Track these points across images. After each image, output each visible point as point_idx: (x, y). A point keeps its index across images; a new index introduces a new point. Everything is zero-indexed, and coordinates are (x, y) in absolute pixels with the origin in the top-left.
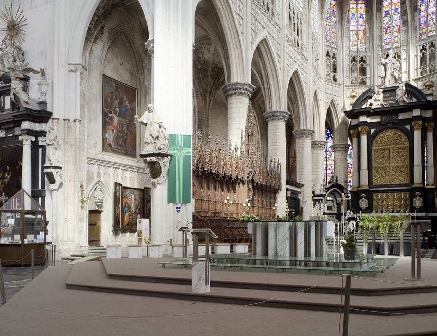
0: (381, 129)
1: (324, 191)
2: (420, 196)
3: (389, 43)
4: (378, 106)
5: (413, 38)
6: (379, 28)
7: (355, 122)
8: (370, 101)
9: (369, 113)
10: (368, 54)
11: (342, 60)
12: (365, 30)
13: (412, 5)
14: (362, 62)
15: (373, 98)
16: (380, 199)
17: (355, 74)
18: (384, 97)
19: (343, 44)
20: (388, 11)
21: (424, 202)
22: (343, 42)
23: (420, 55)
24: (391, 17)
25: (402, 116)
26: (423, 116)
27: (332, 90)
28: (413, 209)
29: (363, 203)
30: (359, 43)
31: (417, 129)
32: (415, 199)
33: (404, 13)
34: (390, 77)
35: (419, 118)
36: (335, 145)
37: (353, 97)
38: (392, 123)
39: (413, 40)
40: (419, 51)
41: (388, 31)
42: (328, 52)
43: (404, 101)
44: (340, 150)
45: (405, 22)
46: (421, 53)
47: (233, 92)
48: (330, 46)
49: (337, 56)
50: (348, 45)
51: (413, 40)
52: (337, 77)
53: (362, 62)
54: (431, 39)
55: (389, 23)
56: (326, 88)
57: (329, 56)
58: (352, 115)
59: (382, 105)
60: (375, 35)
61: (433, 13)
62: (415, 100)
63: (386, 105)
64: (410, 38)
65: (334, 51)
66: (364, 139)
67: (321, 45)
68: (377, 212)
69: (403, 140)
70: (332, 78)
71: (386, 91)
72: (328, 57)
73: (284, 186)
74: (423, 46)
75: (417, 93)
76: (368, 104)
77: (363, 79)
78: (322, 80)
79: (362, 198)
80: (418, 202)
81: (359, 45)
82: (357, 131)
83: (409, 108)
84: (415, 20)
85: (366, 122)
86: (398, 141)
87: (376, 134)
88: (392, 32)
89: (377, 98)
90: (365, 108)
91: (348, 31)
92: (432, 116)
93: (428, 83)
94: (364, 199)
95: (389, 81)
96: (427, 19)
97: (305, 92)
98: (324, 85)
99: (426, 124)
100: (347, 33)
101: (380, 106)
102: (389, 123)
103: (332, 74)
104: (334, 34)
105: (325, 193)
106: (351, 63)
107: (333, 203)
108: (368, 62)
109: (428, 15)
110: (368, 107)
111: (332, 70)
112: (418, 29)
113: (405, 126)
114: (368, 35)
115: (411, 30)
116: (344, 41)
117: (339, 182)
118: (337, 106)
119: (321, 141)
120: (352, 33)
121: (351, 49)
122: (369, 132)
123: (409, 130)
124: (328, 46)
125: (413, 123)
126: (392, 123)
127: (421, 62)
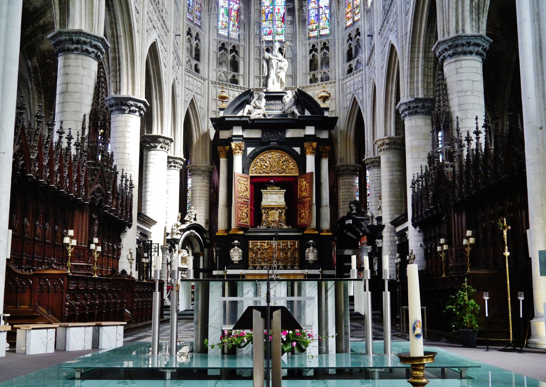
0: (262, 148)
2: (314, 247)
3: (270, 34)
4: (259, 116)
5: (300, 33)
6: (257, 11)
7: (224, 135)
8: (248, 107)
9: (247, 124)
10: (242, 43)
11: (207, 45)
12: (238, 11)
14: (234, 53)
15: (252, 103)
16: (259, 249)
17: (225, 69)
18: (266, 104)
19: (209, 22)
21: (319, 255)
22: (210, 19)
23: (309, 57)
25: (290, 134)
26: (317, 136)
27: (193, 85)
28: (304, 264)
29: (236, 255)
30: (231, 26)
31: (311, 153)
32: (307, 251)
34: (275, 78)
39: (300, 35)
40: (308, 53)
42: (189, 29)
43: (293, 113)
44: (200, 174)
45: (290, 11)
46: (311, 55)
47: (73, 47)
48: (192, 22)
49: (201, 37)
50: (216, 25)
51: (300, 35)
52: (200, 67)
53: (234, 53)
54: (324, 40)
56: (185, 80)
57: (191, 36)
59: (264, 115)
60: (252, 20)
61: (325, 7)
62: (307, 113)
63: (269, 115)
64: (297, 33)
65: (197, 28)
67: (182, 16)
68: (255, 268)
69: (292, 167)
70: (193, 67)
72: (189, 36)
73: (135, 223)
74: (314, 46)
77: (234, 76)
78: (180, 68)
79: (233, 246)
80: (311, 255)
81: (230, 29)
84: (303, 10)
86: (284, 167)
87: (254, 155)
88: (273, 21)
89: (258, 104)
91: (216, 7)
94: (236, 247)
95: (273, 84)
97: (164, 78)
98: (184, 74)
100: (215, 8)
104: (199, 6)
105: (178, 237)
106: (219, 51)
107: (188, 253)
108: (241, 54)
109: (319, 8)
110: (245, 114)
111: (194, 56)
112: (307, 23)
113: (294, 148)
114: (242, 17)
115: (299, 22)
116: (212, 18)
117: (198, 222)
118: (199, 109)
119: (176, 158)
120: (222, 11)
121: (221, 32)
122: (245, 151)
123: (299, 153)
124: (189, 19)
125: (306, 145)
127: (311, 65)
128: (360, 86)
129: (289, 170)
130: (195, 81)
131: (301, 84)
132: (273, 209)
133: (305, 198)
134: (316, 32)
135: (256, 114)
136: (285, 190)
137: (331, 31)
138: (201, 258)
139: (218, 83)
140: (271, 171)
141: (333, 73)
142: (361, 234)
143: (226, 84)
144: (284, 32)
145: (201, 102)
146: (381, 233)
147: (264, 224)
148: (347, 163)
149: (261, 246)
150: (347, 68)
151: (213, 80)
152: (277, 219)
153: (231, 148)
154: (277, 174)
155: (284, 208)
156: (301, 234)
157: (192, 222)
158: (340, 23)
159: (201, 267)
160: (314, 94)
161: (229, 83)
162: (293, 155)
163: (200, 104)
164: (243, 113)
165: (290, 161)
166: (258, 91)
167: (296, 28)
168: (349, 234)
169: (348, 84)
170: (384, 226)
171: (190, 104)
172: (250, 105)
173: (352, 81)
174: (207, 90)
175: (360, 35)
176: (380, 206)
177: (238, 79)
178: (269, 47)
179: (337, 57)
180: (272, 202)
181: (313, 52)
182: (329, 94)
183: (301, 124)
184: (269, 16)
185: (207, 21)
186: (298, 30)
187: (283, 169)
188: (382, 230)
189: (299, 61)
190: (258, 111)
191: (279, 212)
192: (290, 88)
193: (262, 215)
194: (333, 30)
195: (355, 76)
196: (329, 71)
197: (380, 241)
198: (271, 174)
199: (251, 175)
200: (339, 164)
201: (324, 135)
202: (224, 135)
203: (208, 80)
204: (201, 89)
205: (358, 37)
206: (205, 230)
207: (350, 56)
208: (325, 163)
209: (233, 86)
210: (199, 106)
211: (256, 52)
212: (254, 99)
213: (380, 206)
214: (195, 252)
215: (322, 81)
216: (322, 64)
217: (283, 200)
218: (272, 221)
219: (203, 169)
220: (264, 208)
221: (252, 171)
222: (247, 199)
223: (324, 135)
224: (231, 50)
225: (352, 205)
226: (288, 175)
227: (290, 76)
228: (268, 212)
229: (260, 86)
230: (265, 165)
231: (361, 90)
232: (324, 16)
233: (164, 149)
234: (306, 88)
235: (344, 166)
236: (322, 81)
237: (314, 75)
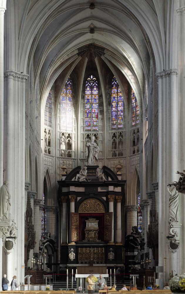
1: (41, 245)
2: (113, 252)
7: (65, 190)
8: (78, 175)
9: (78, 184)
13: (107, 100)
14: (69, 139)
15: (80, 173)
18: (88, 173)
20: (89, 99)
24: (92, 104)
25: (100, 190)
28: (107, 261)
32: (109, 254)
33: (101, 104)
35: (113, 193)
36: (48, 206)
37: (64, 169)
38: (93, 194)
40: (111, 138)
41: (89, 116)
42: (45, 130)
43: (102, 178)
45: (102, 112)
46: (113, 139)
49: (51, 132)
52: (51, 150)
54: (120, 131)
55: (90, 109)
58: (62, 184)
59: (86, 179)
63: (89, 180)
64: (105, 126)
66: (73, 205)
68: (82, 263)
70: (47, 151)
71: (90, 168)
74: (114, 134)
75: (112, 174)
76: (77, 178)
80: (111, 256)
82: (66, 197)
83: (106, 184)
85: (75, 191)
89: (83, 173)
90: (75, 181)
92: (121, 191)
93: (119, 167)
94: (72, 253)
95: (92, 160)
96: (117, 113)
99: (117, 197)
101: (85, 180)
102: (91, 194)
103: (47, 148)
110: (76, 180)
111: (48, 144)
113: (102, 197)
115: (106, 119)
122: (76, 199)
125: (109, 196)
126: (93, 194)
128: (139, 163)
129: (100, 209)
130: (48, 159)
131: (107, 156)
132: (91, 231)
133: (108, 226)
134: (116, 126)
135: (82, 179)
136: (98, 221)
137: (124, 126)
138: (53, 257)
139: (61, 157)
140: (90, 210)
141: (125, 151)
142: (138, 244)
143: (65, 158)
144: (98, 125)
145: (51, 170)
146: (144, 247)
147: (86, 239)
148: (131, 205)
149: (85, 251)
150: (132, 149)
151: (58, 156)
152: (93, 236)
153: (68, 198)
154: (93, 212)
155: (97, 230)
156: (106, 245)
157: (48, 238)
158: (129, 122)
159: (53, 262)
160: (114, 163)
161: (67, 157)
162: (102, 201)
163: (52, 172)
164: (75, 179)
165: (101, 204)
166: (83, 160)
167: (104, 123)
168: (132, 244)
169: (133, 159)
170: (145, 243)
171: (46, 173)
172: (79, 173)
173: (135, 158)
174: (54, 162)
175: (139, 133)
176: (144, 233)
177: (72, 154)
178: (89, 134)
179: (127, 143)
180: (91, 227)
181: (114, 138)
182: (122, 166)
183: (106, 184)
184: (89, 115)
185: (54, 122)
186: (105, 124)
187: (96, 209)
188: (144, 245)
189: (106, 143)
190: (84, 177)
191: (94, 233)
192: (101, 159)
193: (85, 234)
194: (125, 125)
195: (136, 156)
196: (123, 150)
197: (143, 250)
198: (90, 212)
199: (79, 212)
200: (127, 205)
201: (118, 189)
202: (65, 190)
203: (55, 157)
204: (51, 162)
205: (138, 133)
206: (54, 242)
207: (134, 144)
208: (119, 205)
209: (69, 158)
210: (50, 172)
211: (82, 137)
212: (81, 170)
213: (144, 233)
214: (49, 254)
215: (119, 155)
216: (119, 144)
217: (97, 226)
218: (91, 237)
219: (53, 208)
220: (86, 231)
221: (80, 210)
222: (77, 226)
223: (118, 189)
224: (67, 136)
225: (133, 229)
226: (99, 212)
227: (101, 151)
228: (88, 233)
229: (84, 158)
230: (87, 207)
231: (139, 164)
232: (120, 116)
233: (38, 206)
234: (110, 159)
235: (130, 206)
236: (119, 156)
237: (114, 152)
